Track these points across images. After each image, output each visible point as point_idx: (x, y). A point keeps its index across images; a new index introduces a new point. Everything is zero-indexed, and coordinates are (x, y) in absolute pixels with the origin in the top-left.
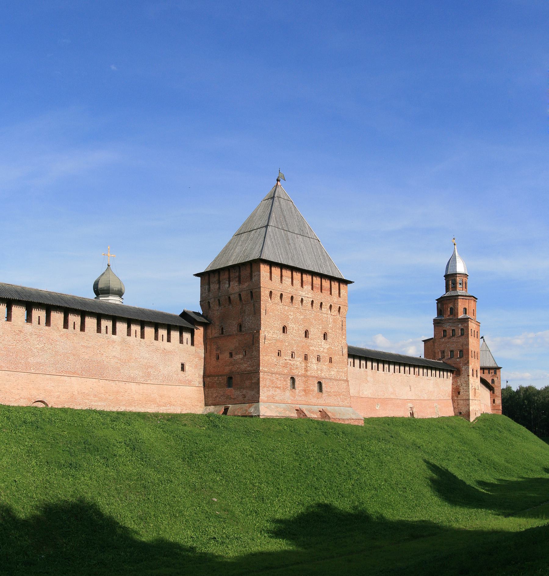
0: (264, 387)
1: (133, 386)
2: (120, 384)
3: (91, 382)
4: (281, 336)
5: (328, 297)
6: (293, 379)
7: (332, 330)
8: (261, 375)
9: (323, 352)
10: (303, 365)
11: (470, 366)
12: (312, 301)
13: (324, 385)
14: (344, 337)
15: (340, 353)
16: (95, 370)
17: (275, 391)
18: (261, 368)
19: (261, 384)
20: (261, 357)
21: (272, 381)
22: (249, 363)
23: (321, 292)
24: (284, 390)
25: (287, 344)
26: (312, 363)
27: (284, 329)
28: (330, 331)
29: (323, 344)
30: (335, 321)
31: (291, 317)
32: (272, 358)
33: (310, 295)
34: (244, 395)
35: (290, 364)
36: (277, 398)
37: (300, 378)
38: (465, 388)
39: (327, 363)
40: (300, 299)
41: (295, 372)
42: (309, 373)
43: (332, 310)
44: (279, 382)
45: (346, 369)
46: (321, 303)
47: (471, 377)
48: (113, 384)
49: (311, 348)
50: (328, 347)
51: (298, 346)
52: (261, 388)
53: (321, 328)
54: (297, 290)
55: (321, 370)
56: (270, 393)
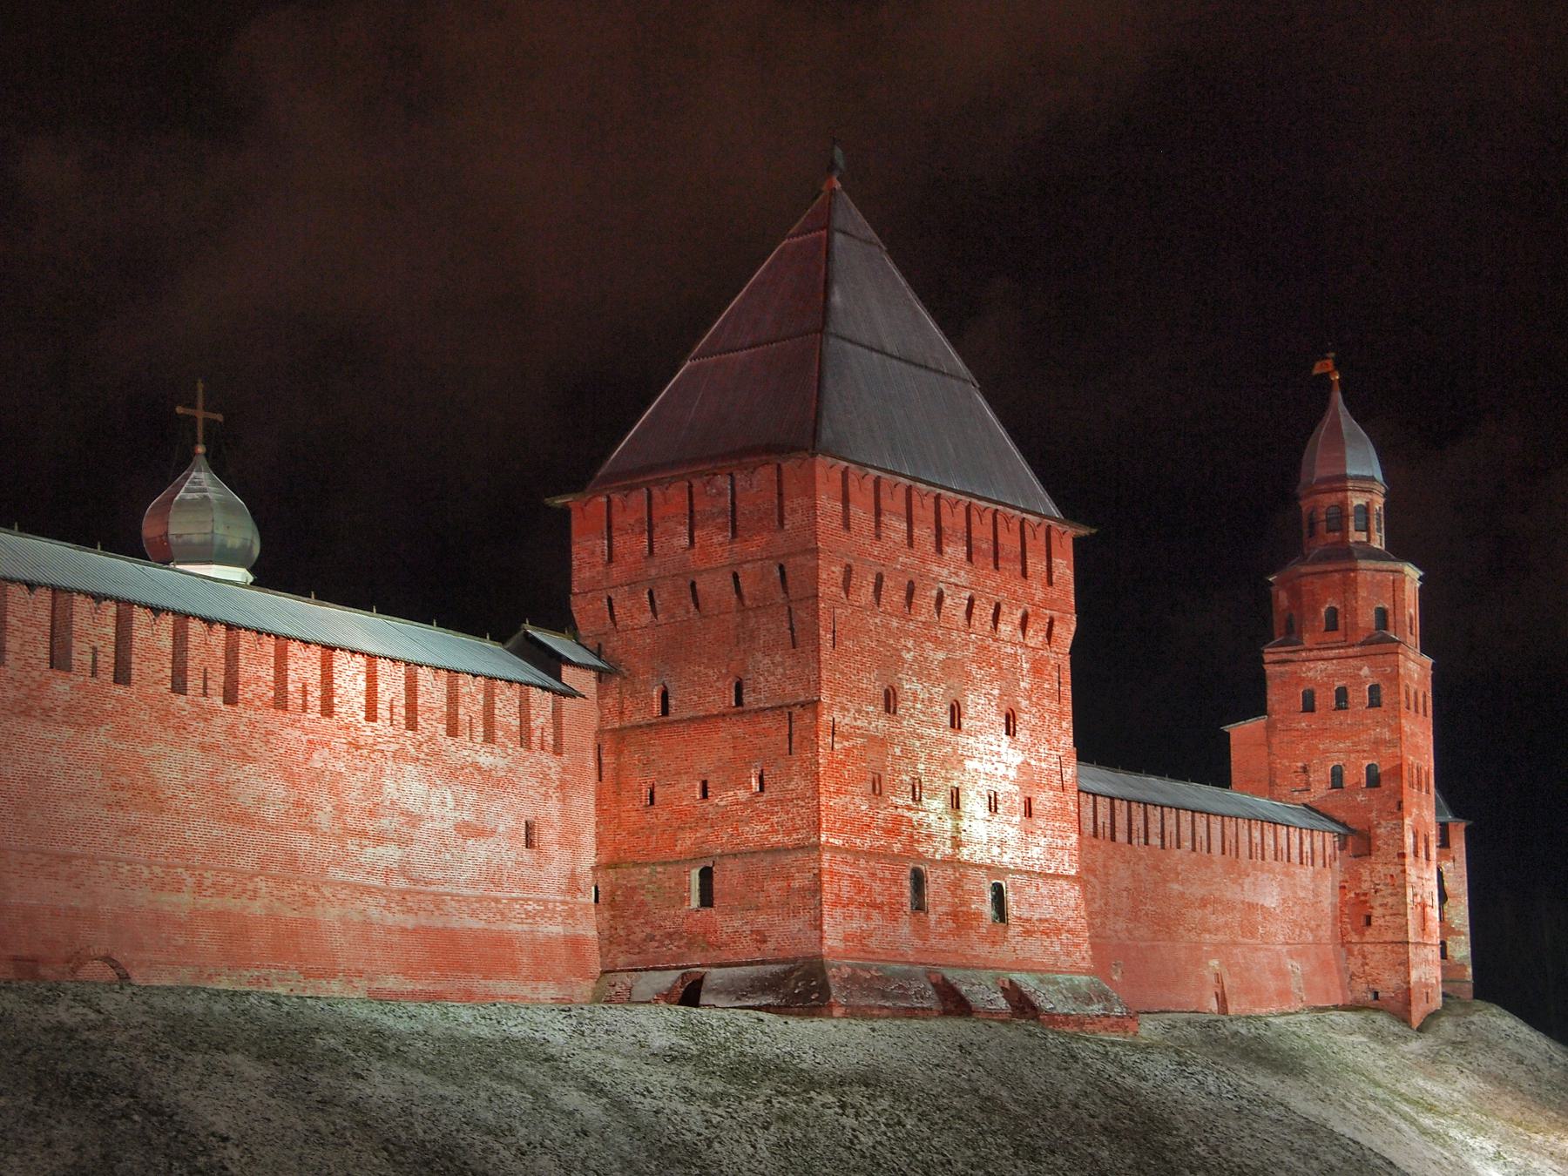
5: (1018, 586)
7: (1029, 698)
9: (1005, 777)
11: (1407, 821)
13: (1010, 896)
22: (775, 819)
23: (997, 567)
26: (973, 818)
28: (1024, 703)
29: (1003, 749)
31: (908, 656)
32: (857, 800)
33: (963, 578)
34: (758, 932)
38: (1390, 900)
39: (1017, 819)
40: (935, 593)
42: (964, 853)
43: (1030, 633)
47: (1409, 860)
49: (969, 765)
51: (930, 756)
53: (996, 692)
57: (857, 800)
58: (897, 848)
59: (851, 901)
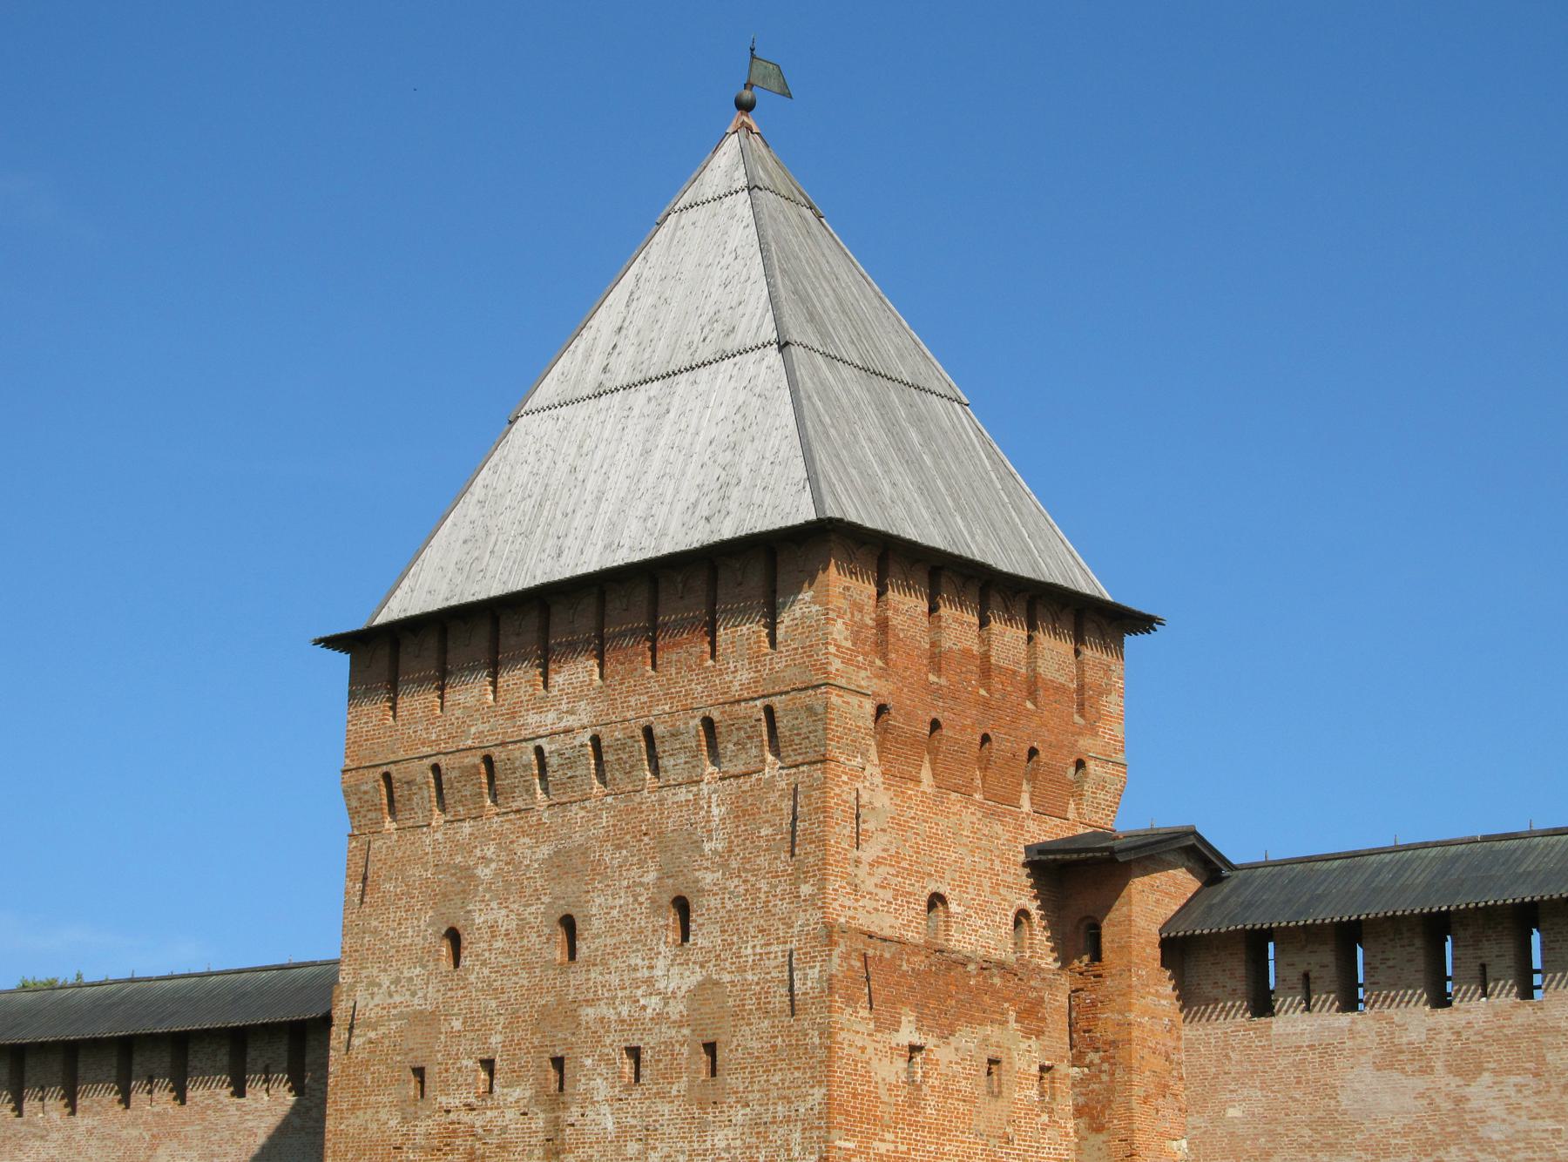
7: (724, 866)
9: (659, 1018)
10: (539, 1121)
14: (806, 889)
15: (779, 999)
20: (330, 1124)
25: (457, 1024)
26: (588, 1099)
28: (708, 878)
29: (658, 972)
30: (741, 812)
31: (485, 873)
32: (383, 1116)
43: (727, 747)
45: (819, 1093)
49: (588, 1014)
50: (695, 977)
53: (651, 877)
57: (383, 1116)
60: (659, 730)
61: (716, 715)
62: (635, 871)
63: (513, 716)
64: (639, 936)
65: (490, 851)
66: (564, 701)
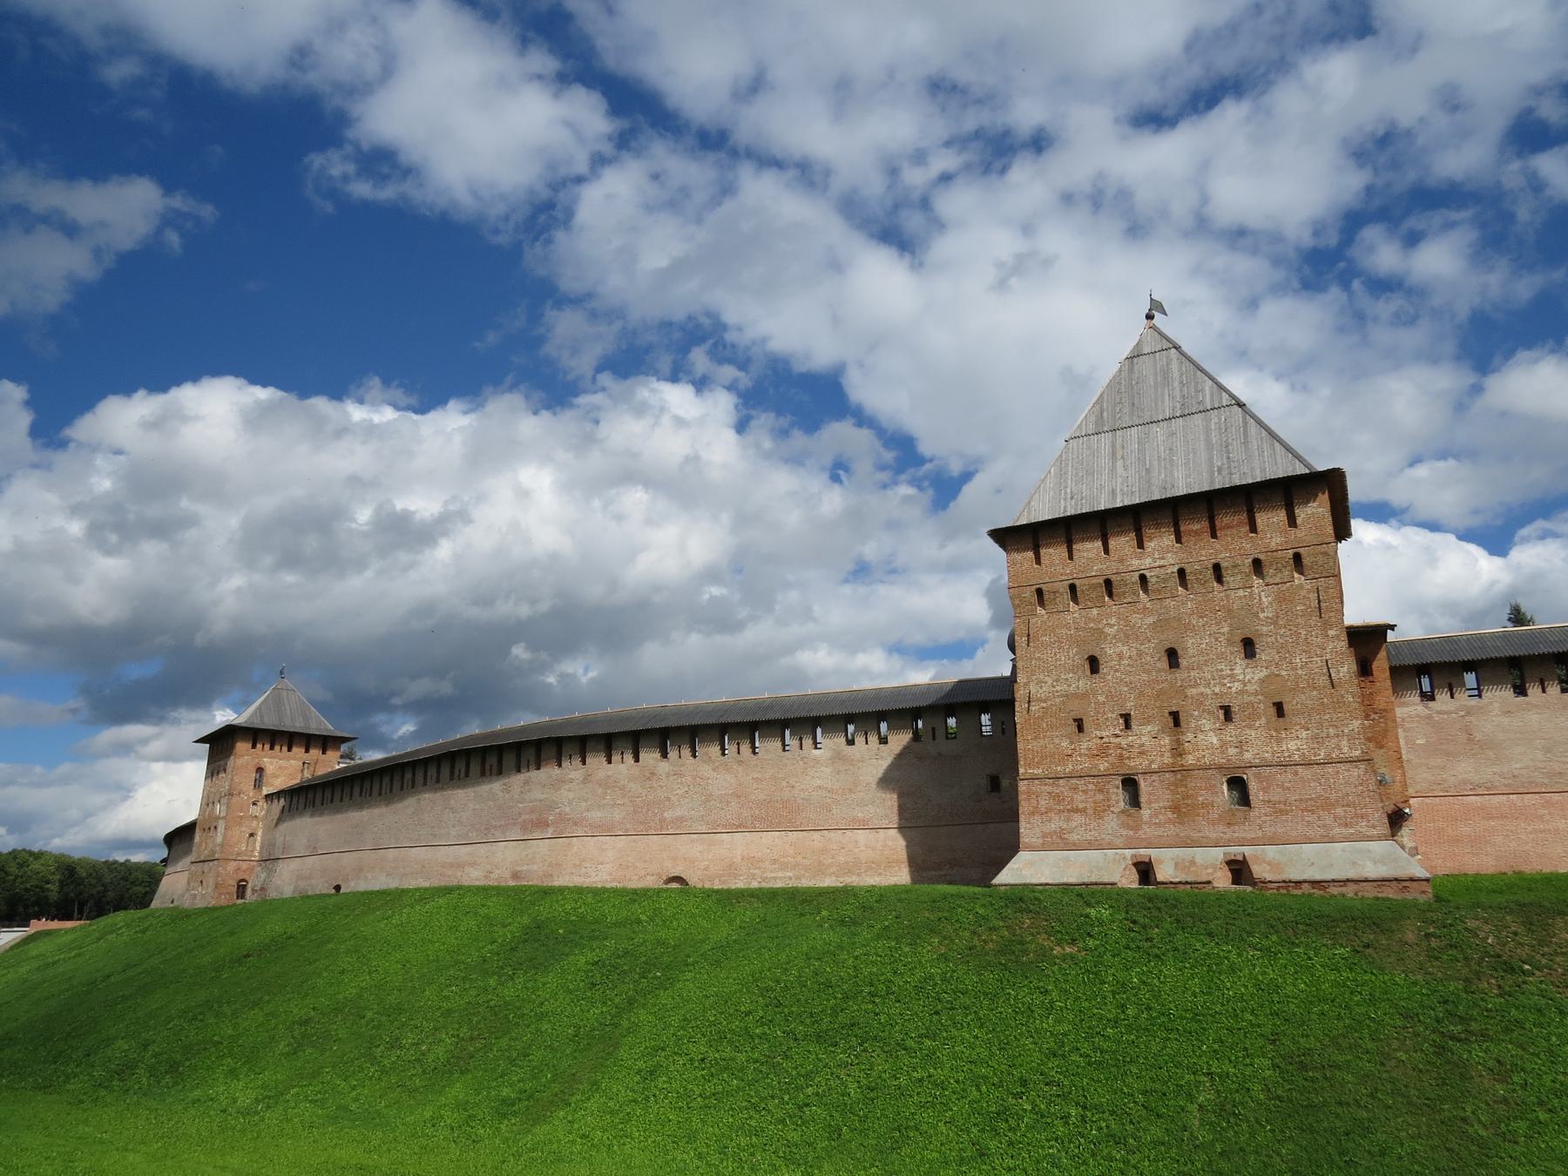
0: (1033, 813)
1: (862, 836)
2: (832, 834)
3: (768, 839)
4: (1083, 683)
6: (1130, 784)
7: (1275, 623)
8: (1022, 786)
9: (1241, 692)
10: (1166, 741)
12: (1181, 572)
13: (1253, 787)
16: (778, 816)
17: (1068, 820)
18: (1021, 771)
19: (1024, 807)
21: (1058, 798)
24: (1099, 812)
25: (1101, 699)
27: (1094, 664)
29: (1237, 671)
30: (1280, 599)
35: (1119, 746)
36: (1074, 837)
37: (1155, 777)
41: (1136, 764)
42: (1190, 760)
44: (1080, 797)
46: (1217, 568)
48: (816, 835)
51: (1141, 694)
52: (1022, 818)
53: (1226, 629)
54: (1121, 561)
55: (1240, 745)
56: (1053, 826)
58: (1103, 766)
59: (1049, 810)
60: (1224, 565)
61: (1262, 557)
62: (1214, 628)
63: (1121, 561)
64: (1221, 656)
65: (1113, 621)
66: (1161, 552)
